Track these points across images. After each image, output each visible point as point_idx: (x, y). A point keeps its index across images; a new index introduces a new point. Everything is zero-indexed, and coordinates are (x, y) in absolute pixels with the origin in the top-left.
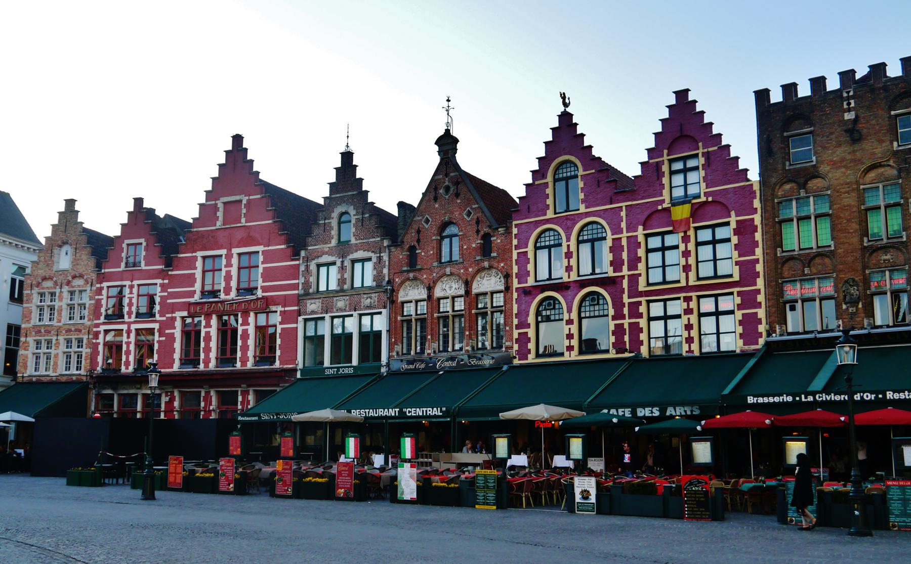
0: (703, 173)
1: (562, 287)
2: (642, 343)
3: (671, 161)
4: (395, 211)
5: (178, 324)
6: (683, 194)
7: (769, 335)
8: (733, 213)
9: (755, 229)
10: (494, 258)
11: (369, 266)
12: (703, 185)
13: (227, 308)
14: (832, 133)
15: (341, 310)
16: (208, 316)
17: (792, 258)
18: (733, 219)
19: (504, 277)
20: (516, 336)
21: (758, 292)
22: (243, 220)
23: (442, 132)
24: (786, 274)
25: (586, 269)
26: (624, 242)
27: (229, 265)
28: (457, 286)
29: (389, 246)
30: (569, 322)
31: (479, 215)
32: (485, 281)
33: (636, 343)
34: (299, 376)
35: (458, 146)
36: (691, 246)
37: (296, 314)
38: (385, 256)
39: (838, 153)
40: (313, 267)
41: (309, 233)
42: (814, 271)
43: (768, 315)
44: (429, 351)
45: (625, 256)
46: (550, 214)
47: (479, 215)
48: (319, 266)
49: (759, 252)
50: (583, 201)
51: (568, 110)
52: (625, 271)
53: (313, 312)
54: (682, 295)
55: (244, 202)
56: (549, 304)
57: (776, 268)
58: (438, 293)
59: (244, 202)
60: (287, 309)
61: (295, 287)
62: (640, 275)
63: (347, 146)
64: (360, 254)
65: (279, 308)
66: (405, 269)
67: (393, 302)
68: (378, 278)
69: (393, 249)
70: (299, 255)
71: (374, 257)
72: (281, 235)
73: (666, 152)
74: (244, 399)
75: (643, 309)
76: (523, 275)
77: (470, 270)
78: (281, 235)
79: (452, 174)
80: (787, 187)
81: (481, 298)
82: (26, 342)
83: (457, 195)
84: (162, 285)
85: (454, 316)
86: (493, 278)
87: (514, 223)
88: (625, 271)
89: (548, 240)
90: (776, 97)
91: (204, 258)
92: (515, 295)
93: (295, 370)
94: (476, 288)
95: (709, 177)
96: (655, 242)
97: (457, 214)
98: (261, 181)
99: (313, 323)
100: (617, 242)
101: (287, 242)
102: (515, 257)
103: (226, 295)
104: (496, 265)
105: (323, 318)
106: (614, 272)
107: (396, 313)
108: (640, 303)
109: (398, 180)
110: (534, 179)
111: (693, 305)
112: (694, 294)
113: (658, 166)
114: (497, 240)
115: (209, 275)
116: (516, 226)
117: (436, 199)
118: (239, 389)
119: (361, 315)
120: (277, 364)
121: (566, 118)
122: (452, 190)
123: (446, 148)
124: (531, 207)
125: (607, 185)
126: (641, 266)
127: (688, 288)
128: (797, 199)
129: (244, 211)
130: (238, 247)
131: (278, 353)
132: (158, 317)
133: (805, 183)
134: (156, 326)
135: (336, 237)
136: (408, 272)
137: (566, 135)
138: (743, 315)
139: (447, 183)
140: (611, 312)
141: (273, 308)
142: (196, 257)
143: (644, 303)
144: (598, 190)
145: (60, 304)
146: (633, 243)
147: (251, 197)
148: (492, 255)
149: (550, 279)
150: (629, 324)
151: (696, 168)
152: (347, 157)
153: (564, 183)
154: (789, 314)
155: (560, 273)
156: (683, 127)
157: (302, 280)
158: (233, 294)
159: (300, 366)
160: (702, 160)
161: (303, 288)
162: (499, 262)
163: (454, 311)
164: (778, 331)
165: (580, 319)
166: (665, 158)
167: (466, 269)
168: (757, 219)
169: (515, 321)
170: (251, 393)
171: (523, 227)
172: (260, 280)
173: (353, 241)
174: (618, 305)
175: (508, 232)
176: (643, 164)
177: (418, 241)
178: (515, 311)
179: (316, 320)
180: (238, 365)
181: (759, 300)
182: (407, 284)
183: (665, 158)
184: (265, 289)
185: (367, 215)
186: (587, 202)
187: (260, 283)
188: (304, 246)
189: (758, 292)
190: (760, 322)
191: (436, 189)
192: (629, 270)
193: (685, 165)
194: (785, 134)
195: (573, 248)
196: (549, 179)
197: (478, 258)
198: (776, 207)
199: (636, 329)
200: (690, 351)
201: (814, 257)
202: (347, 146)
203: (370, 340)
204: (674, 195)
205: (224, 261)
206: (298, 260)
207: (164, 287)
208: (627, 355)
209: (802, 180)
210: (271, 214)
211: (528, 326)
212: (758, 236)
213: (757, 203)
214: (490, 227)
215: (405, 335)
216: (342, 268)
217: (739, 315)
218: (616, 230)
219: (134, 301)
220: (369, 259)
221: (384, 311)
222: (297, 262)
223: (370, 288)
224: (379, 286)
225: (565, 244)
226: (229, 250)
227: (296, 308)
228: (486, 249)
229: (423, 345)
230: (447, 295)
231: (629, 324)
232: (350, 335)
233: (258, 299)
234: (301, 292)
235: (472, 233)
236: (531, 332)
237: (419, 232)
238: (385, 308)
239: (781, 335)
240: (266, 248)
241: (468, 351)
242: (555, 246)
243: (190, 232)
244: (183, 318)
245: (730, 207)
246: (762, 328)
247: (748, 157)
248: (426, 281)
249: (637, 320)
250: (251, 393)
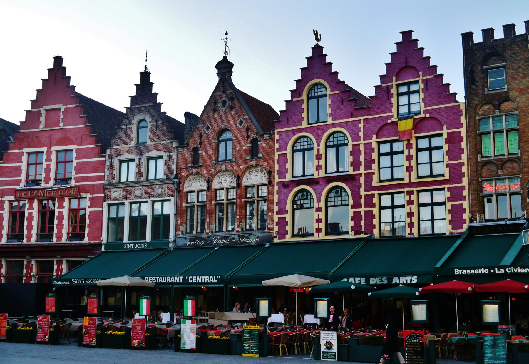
0: (422, 95)
1: (313, 182)
2: (374, 227)
3: (398, 86)
4: (182, 120)
5: (6, 206)
6: (407, 111)
7: (471, 221)
8: (445, 127)
9: (462, 139)
10: (260, 158)
11: (161, 162)
12: (423, 105)
13: (47, 194)
14: (520, 67)
15: (138, 197)
16: (31, 201)
17: (489, 163)
18: (445, 132)
19: (268, 173)
20: (276, 220)
21: (463, 188)
22: (61, 124)
23: (221, 59)
24: (484, 174)
25: (332, 168)
26: (362, 148)
27: (49, 159)
28: (230, 180)
29: (177, 147)
30: (319, 209)
31: (249, 124)
32: (252, 176)
33: (370, 227)
34: (103, 249)
35: (234, 69)
36: (413, 152)
37: (102, 201)
38: (174, 156)
39: (524, 82)
40: (116, 162)
41: (114, 136)
42: (506, 172)
43: (471, 206)
44: (208, 231)
46: (304, 125)
47: (249, 124)
48: (121, 162)
49: (464, 157)
50: (330, 115)
51: (319, 43)
52: (362, 171)
53: (115, 199)
54: (406, 190)
55: (62, 110)
56: (303, 195)
57: (477, 170)
58: (215, 185)
59: (62, 110)
60: (94, 196)
61: (102, 178)
62: (373, 173)
63: (146, 67)
64: (154, 153)
65: (89, 195)
66: (190, 165)
67: (179, 191)
69: (180, 150)
70: (105, 153)
71: (165, 156)
72: (91, 136)
73: (394, 78)
74: (58, 267)
75: (375, 200)
76: (282, 172)
77: (241, 167)
78: (91, 136)
79: (228, 92)
80: (486, 107)
81: (249, 189)
83: (232, 108)
85: (227, 204)
86: (259, 174)
87: (276, 131)
88: (362, 171)
89: (302, 145)
90: (478, 38)
91: (29, 154)
92: (276, 188)
93: (100, 245)
94: (245, 182)
95: (427, 99)
96: (385, 148)
97: (231, 123)
98: (76, 93)
99: (115, 207)
100: (356, 147)
101: (96, 142)
102: (276, 157)
103: (46, 184)
104: (261, 163)
105: (123, 204)
106: (354, 171)
107: (182, 200)
108: (373, 195)
109: (184, 96)
110: (292, 96)
111: (414, 197)
112: (414, 189)
113: (388, 89)
114: (262, 144)
115: (32, 168)
116: (278, 133)
117: (215, 111)
118: (55, 260)
119: (154, 202)
120: (86, 240)
121: (318, 50)
122: (228, 103)
123: (223, 71)
124: (290, 119)
125: (349, 103)
126: (375, 167)
127: (410, 184)
128: (493, 117)
129: (62, 117)
130: (56, 145)
131: (87, 231)
133: (500, 105)
135: (135, 139)
136: (192, 168)
137: (318, 62)
138: (452, 205)
139: (224, 99)
140: (351, 202)
141: (84, 195)
142: (22, 153)
143: (376, 196)
144: (342, 106)
146: (369, 149)
147: (68, 106)
148: (260, 155)
149: (304, 175)
150: (365, 211)
151: (417, 92)
152: (145, 76)
153: (315, 100)
154: (487, 206)
155: (311, 171)
156: (408, 58)
157: (107, 173)
158: (52, 183)
159: (104, 242)
160: (422, 86)
161: (108, 179)
162: (263, 161)
163: (227, 199)
164: (478, 218)
165: (327, 207)
166: (394, 83)
167: (238, 167)
168: (463, 131)
169: (276, 208)
170: (64, 262)
171: (283, 134)
172: (74, 172)
173: (149, 143)
174: (356, 196)
175: (272, 138)
176: (376, 87)
177: (201, 144)
178: (276, 200)
179: (118, 205)
180: (55, 240)
181: (464, 194)
182: (191, 177)
183: (394, 83)
184: (77, 180)
185: (160, 123)
186: (333, 115)
187: (74, 175)
188: (109, 146)
189: (463, 188)
190: (464, 211)
191: (215, 103)
192: (365, 169)
193: (409, 88)
194: (485, 67)
195: (322, 152)
196: (304, 97)
197: (248, 158)
198: (477, 123)
199: (370, 216)
200: (411, 233)
201: (505, 162)
202: (146, 67)
203: (161, 222)
204: (400, 112)
205: (45, 157)
206: (105, 156)
208: (363, 236)
209: (497, 103)
210: (83, 120)
211: (286, 212)
212: (464, 145)
213: (463, 120)
214: (257, 133)
215: (189, 218)
216: (140, 164)
217: (449, 205)
218: (356, 138)
220: (161, 157)
221: (172, 199)
222: (104, 159)
223: (161, 180)
224: (168, 179)
225: (316, 148)
227: (102, 195)
228: (254, 151)
229: (202, 226)
230: (222, 187)
231: (365, 211)
232: (145, 218)
233: (71, 187)
234: (106, 182)
235: (243, 138)
236: (288, 217)
237: (201, 136)
238: (173, 196)
239: (480, 222)
240: (79, 147)
241: (238, 231)
242: (308, 149)
243: (18, 132)
244: (11, 202)
245: (442, 122)
247: (457, 85)
248: (206, 175)
249: (371, 209)
250: (64, 262)
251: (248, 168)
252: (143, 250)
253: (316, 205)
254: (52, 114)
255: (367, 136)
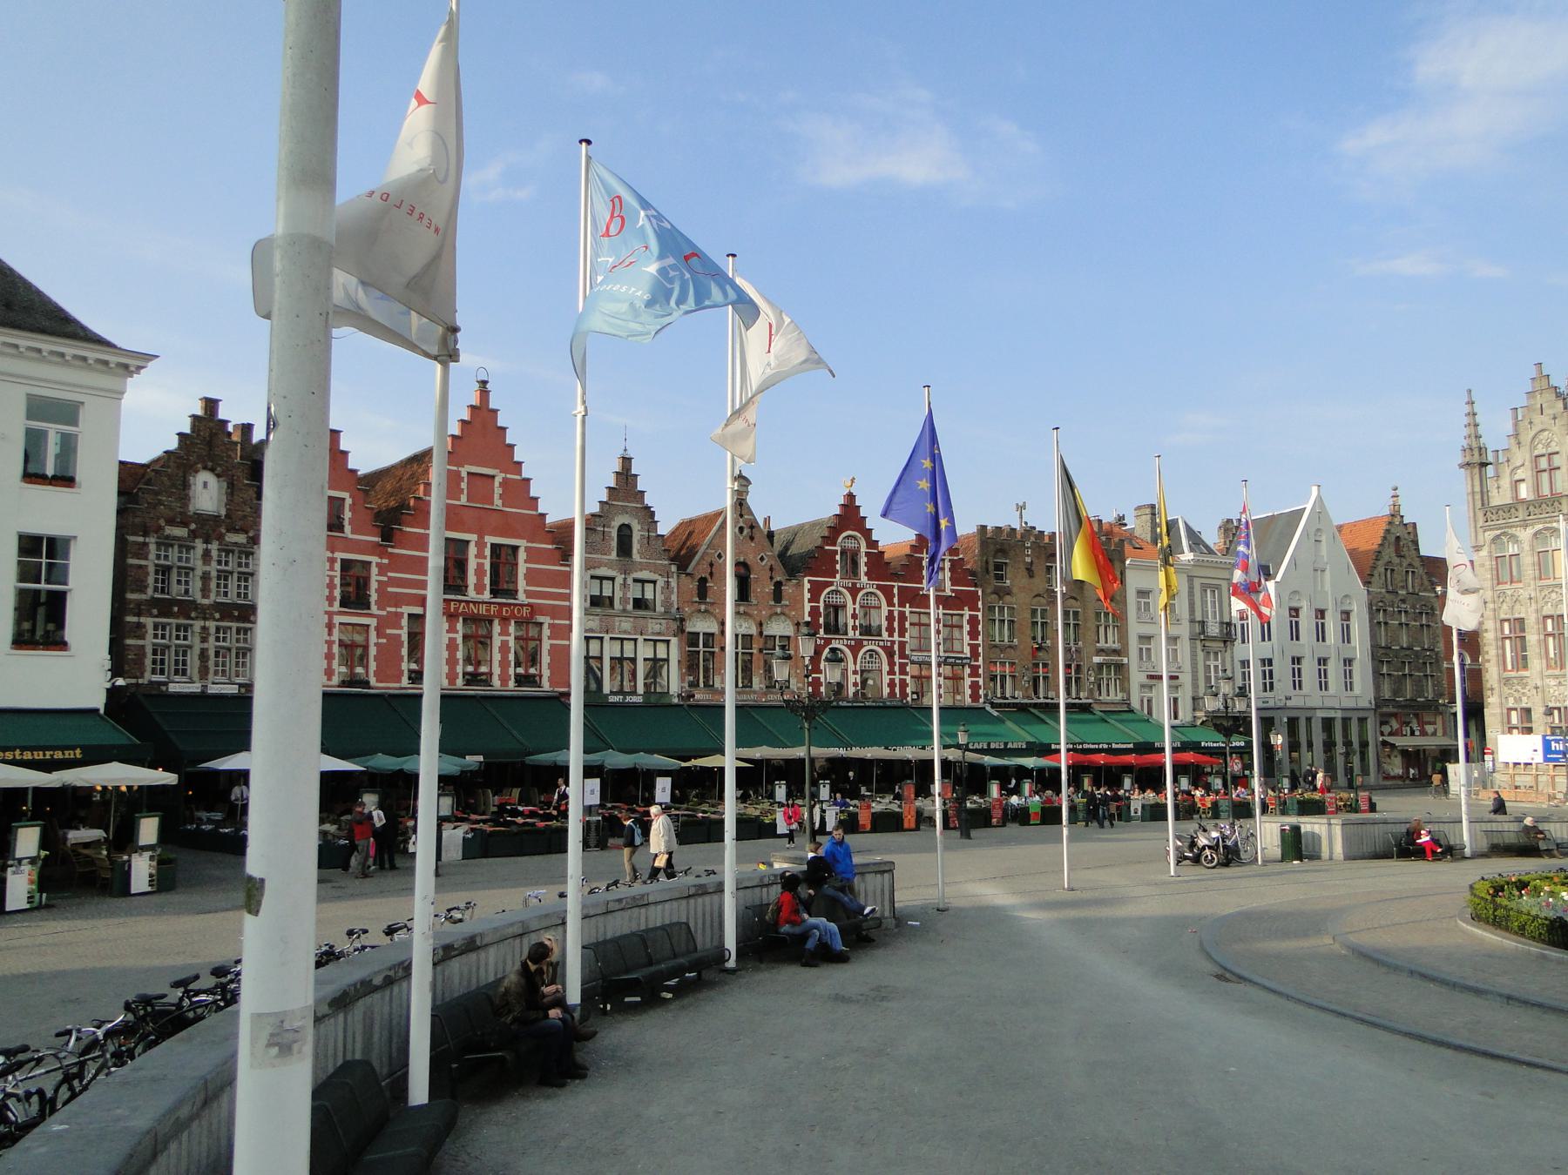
22: (498, 503)
30: (855, 672)
33: (904, 694)
45: (896, 624)
52: (896, 637)
55: (498, 480)
65: (546, 620)
67: (683, 631)
68: (667, 603)
71: (661, 583)
82: (140, 626)
83: (752, 538)
84: (378, 565)
88: (896, 637)
102: (807, 608)
114: (787, 589)
120: (546, 685)
129: (498, 491)
132: (374, 609)
134: (373, 622)
140: (886, 668)
141: (540, 619)
145: (207, 568)
146: (902, 614)
152: (626, 461)
158: (487, 596)
168: (980, 614)
174: (891, 664)
175: (800, 585)
177: (711, 574)
180: (496, 682)
207: (382, 570)
216: (625, 584)
218: (890, 603)
219: (337, 581)
221: (674, 641)
226: (481, 537)
228: (778, 595)
237: (711, 565)
246: (981, 692)
251: (771, 616)
252: (635, 706)
253: (851, 667)
254: (479, 482)
255: (902, 604)
